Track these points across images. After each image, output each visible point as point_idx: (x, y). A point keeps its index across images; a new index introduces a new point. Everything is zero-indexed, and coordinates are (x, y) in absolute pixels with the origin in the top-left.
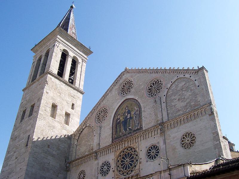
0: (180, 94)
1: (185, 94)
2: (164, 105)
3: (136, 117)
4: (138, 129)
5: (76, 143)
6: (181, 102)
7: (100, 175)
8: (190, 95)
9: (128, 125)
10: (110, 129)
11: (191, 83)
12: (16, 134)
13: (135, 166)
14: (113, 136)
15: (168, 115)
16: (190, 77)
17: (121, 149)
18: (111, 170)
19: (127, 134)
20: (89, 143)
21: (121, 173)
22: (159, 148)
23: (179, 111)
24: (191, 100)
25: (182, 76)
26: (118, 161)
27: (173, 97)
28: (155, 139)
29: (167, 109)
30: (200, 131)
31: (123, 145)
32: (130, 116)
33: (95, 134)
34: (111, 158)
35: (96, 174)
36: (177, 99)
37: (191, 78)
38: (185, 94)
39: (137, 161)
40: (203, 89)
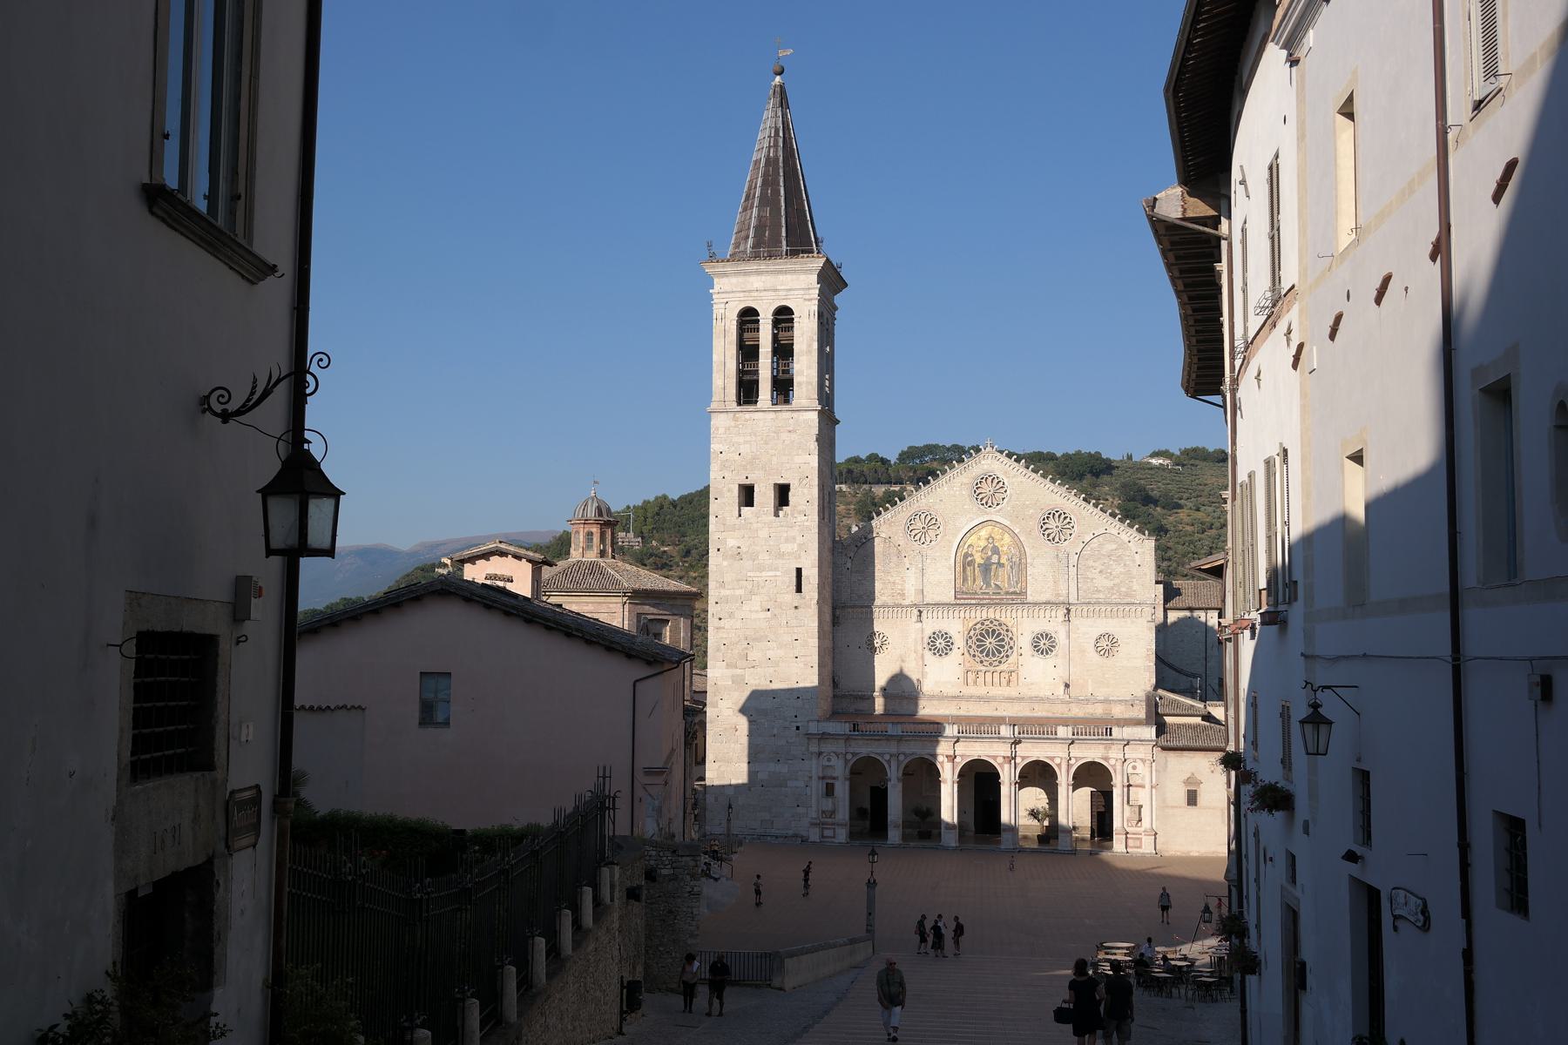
0: (1105, 563)
1: (1114, 567)
2: (1073, 571)
3: (1011, 567)
5: (849, 565)
7: (928, 655)
8: (1121, 573)
10: (950, 569)
12: (732, 542)
13: (1007, 656)
17: (979, 619)
18: (955, 649)
20: (892, 580)
21: (977, 659)
22: (1057, 641)
25: (1115, 532)
26: (971, 638)
27: (1091, 563)
28: (1051, 622)
30: (1128, 638)
31: (984, 613)
34: (956, 626)
35: (920, 648)
36: (1098, 570)
38: (1114, 567)
39: (1011, 648)
40: (1145, 574)
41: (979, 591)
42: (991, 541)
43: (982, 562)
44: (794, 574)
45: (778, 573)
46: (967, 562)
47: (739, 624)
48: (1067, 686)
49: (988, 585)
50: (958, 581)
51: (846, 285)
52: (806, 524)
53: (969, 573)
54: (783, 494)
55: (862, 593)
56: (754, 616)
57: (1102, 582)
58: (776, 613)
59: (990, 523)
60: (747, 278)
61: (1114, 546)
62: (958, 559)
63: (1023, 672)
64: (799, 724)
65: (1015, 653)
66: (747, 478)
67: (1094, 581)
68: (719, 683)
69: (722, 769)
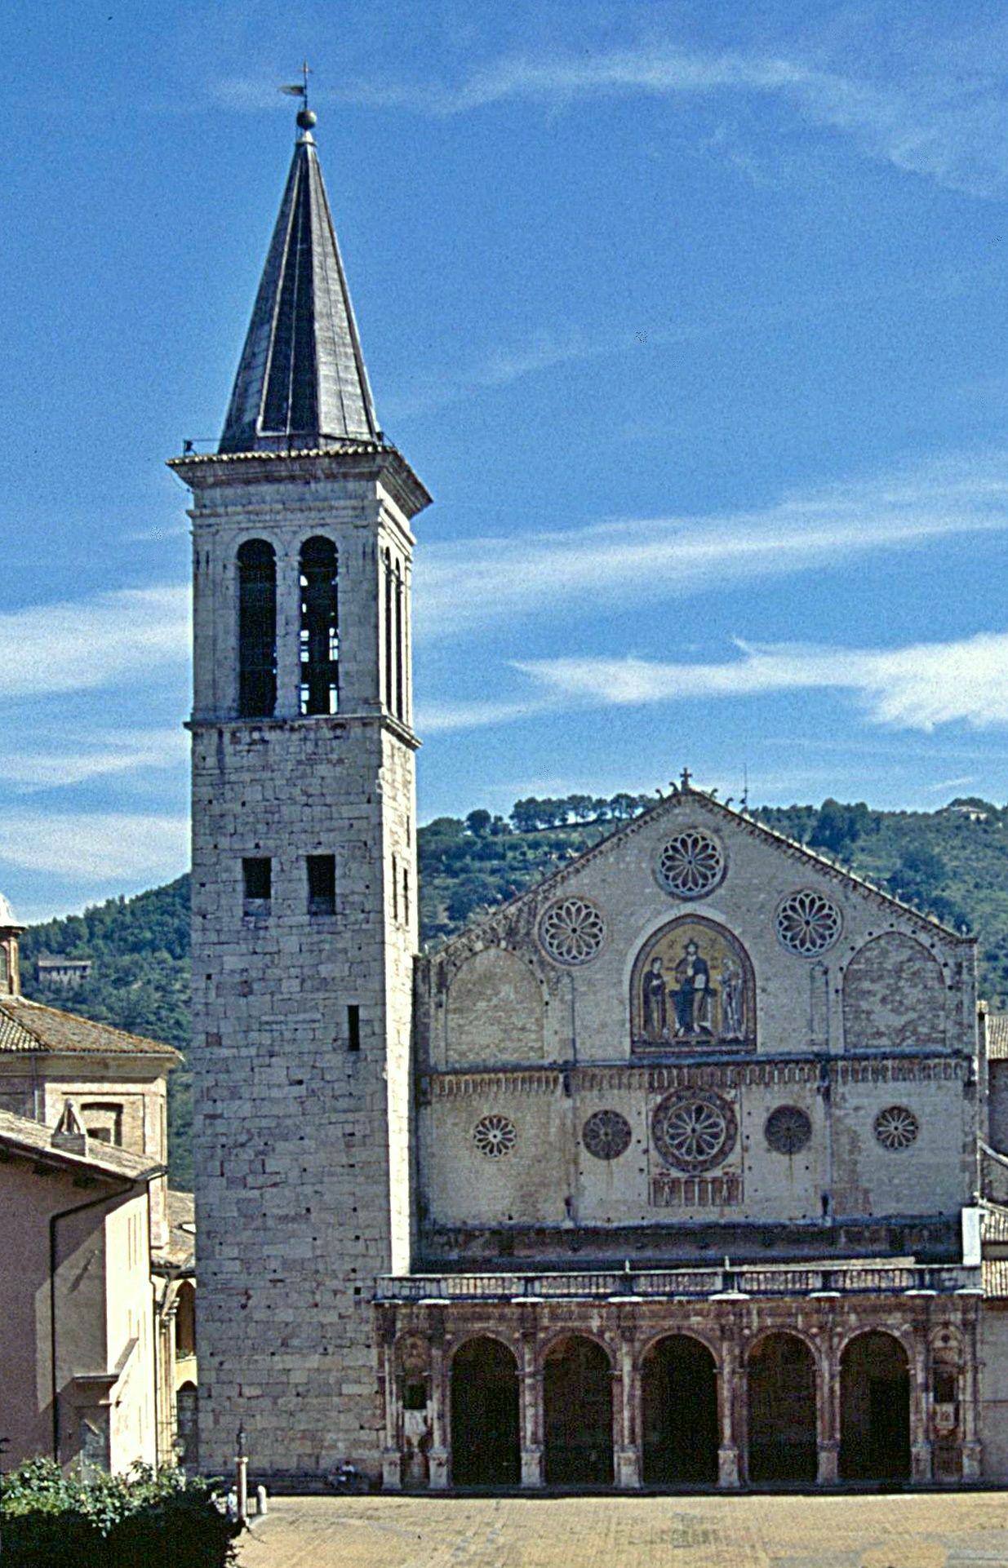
3: (729, 995)
4: (736, 1041)
6: (892, 1010)
8: (919, 1001)
9: (696, 1013)
10: (622, 1002)
11: (930, 965)
12: (231, 962)
14: (636, 1031)
15: (845, 1031)
16: (933, 946)
19: (693, 1043)
23: (880, 1034)
24: (920, 1018)
25: (906, 929)
27: (866, 985)
29: (844, 1012)
32: (707, 981)
33: (546, 998)
36: (879, 996)
37: (934, 951)
38: (906, 991)
41: (673, 1041)
42: (692, 949)
43: (677, 987)
44: (344, 1017)
45: (319, 1016)
46: (649, 992)
47: (247, 1109)
48: (825, 1201)
49: (689, 1029)
50: (636, 1021)
51: (430, 501)
52: (364, 926)
53: (654, 1005)
54: (321, 872)
55: (464, 1047)
56: (275, 1093)
57: (885, 1018)
58: (314, 1086)
59: (688, 920)
60: (252, 489)
61: (906, 953)
62: (636, 984)
63: (749, 1182)
64: (359, 1284)
65: (738, 1147)
66: (257, 846)
67: (872, 1017)
68: (215, 1214)
69: (226, 1366)
